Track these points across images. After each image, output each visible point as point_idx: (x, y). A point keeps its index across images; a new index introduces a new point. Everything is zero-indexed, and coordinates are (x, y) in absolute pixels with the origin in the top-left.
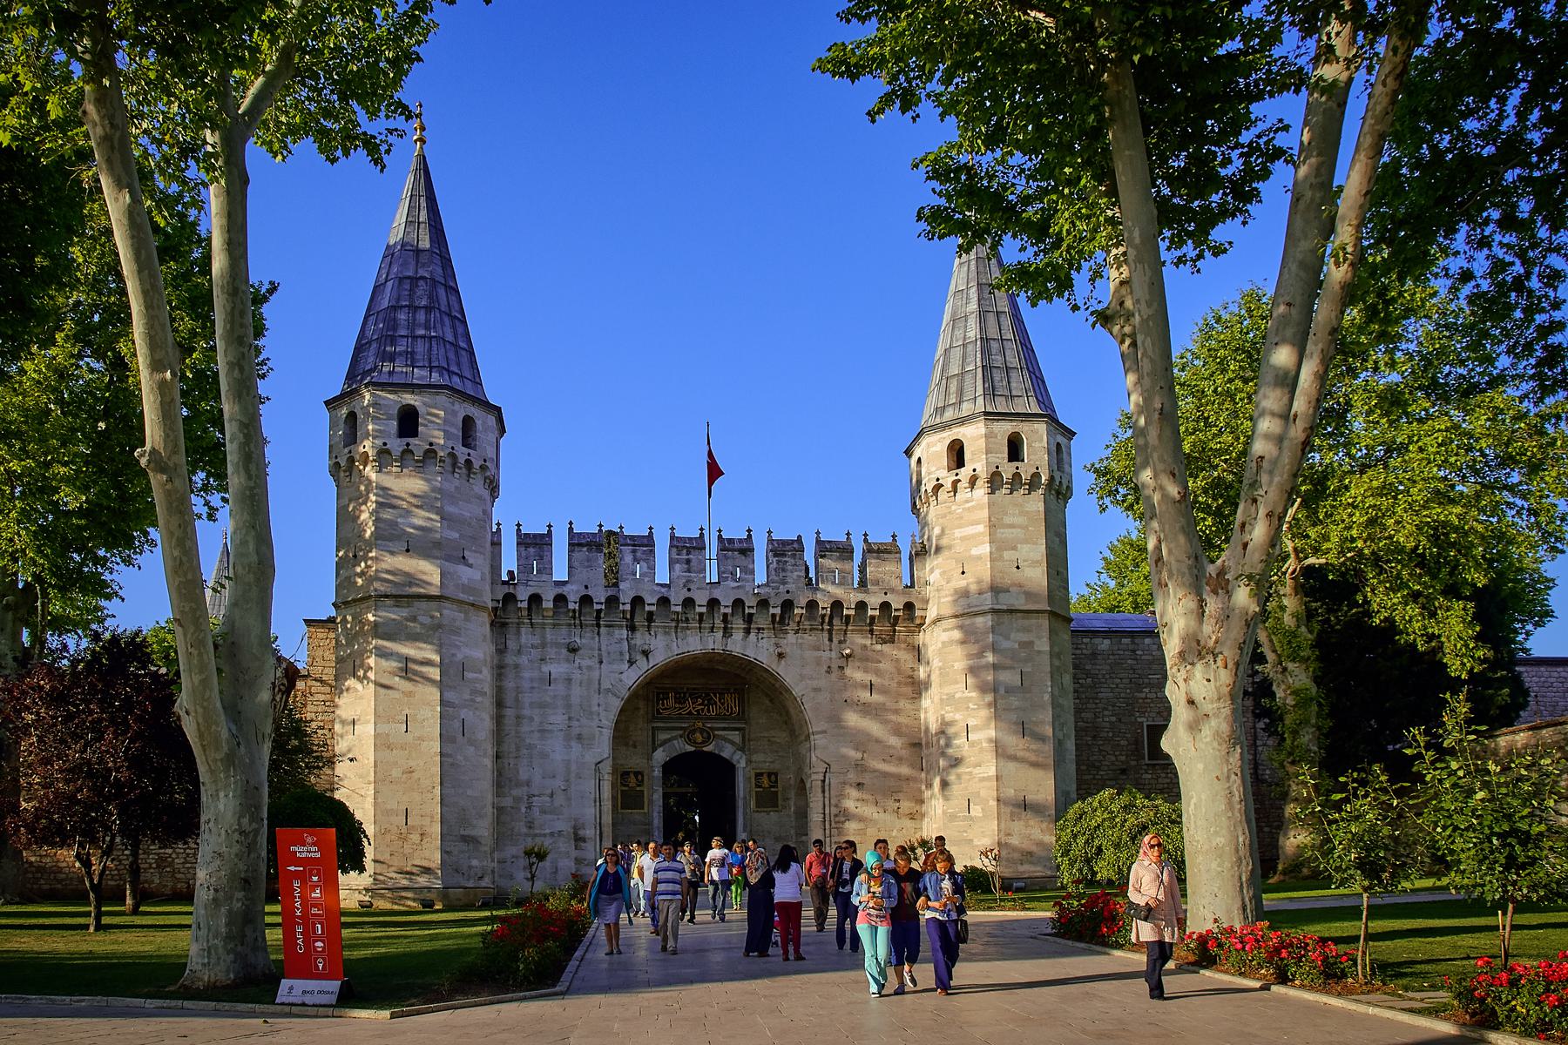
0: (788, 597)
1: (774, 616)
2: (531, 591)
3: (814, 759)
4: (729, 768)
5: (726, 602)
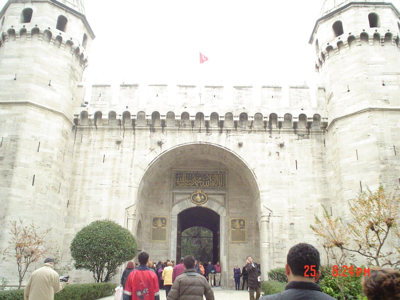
1: (236, 122)
2: (97, 110)
3: (262, 208)
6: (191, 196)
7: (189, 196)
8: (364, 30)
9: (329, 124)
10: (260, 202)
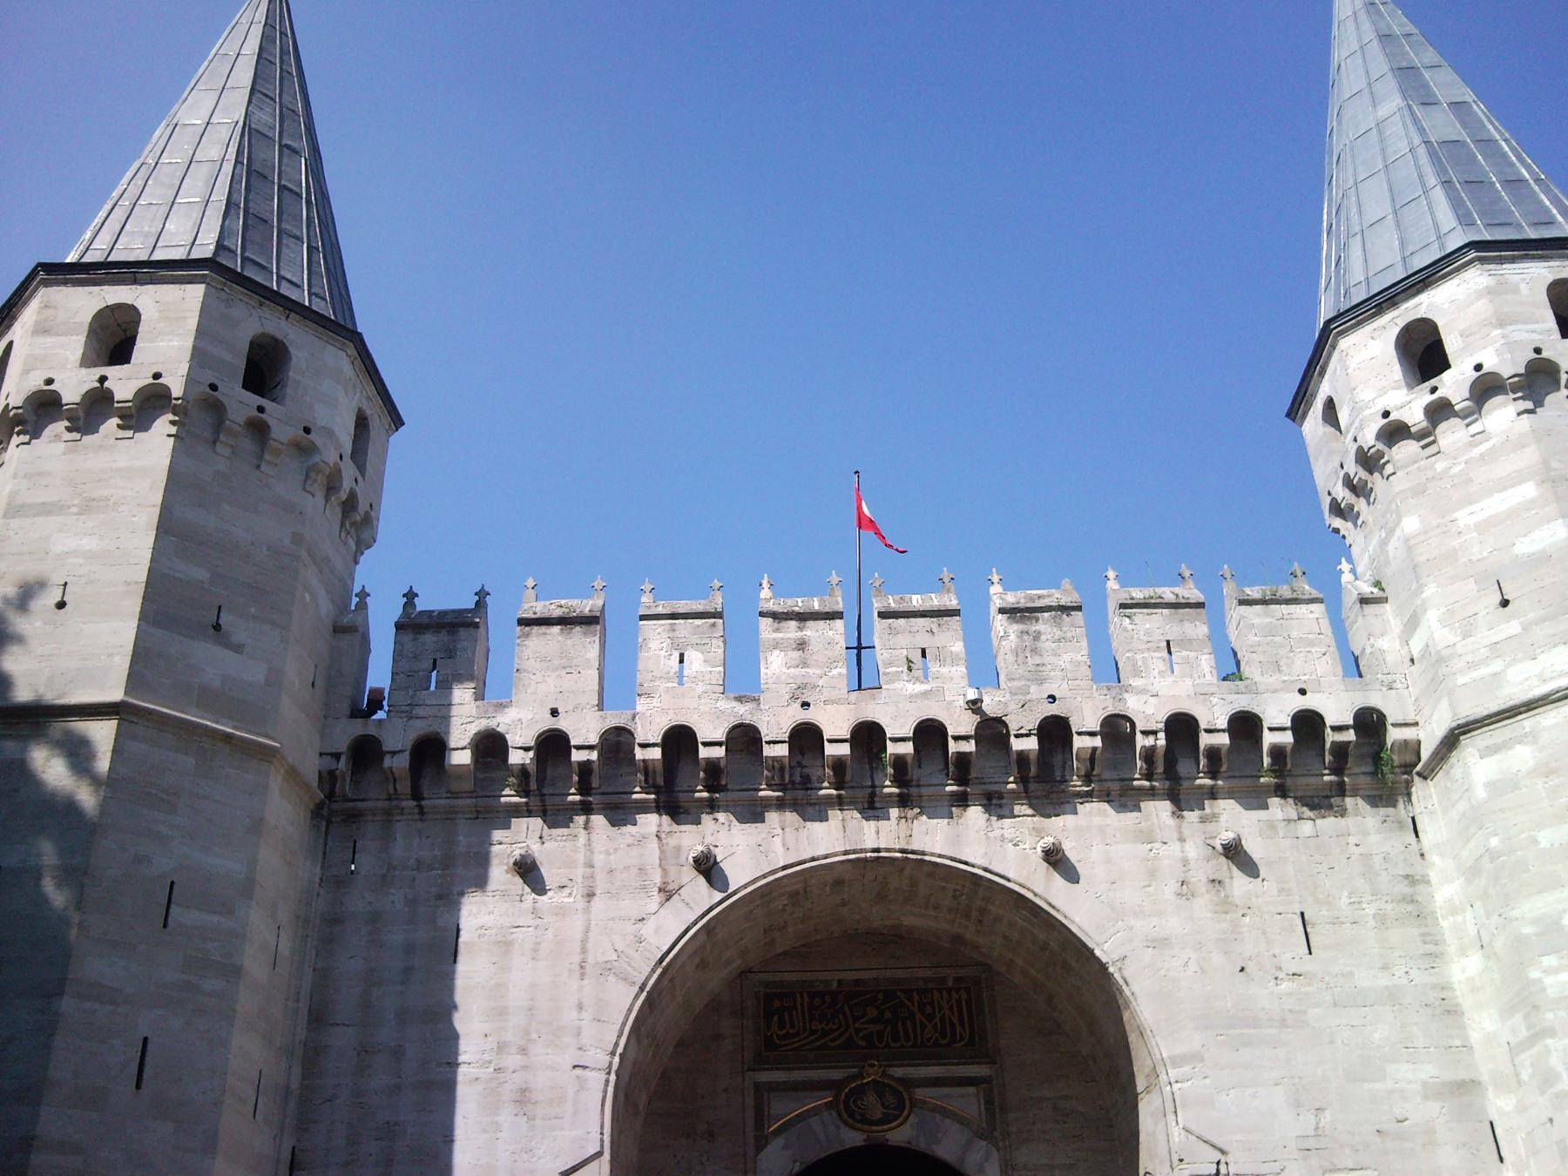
0: (1054, 710)
1: (1022, 757)
2: (418, 729)
5: (898, 724)
6: (837, 1097)
8: (1538, 351)
9: (1425, 754)
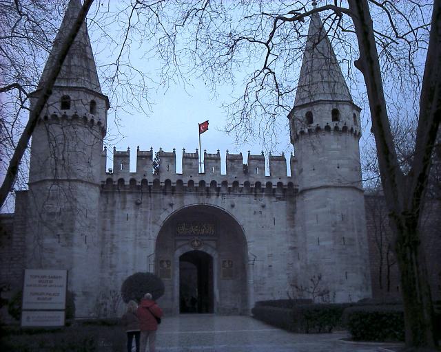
0: (237, 180)
2: (120, 177)
4: (209, 258)
5: (208, 181)
7: (188, 242)
9: (299, 191)
10: (247, 250)
